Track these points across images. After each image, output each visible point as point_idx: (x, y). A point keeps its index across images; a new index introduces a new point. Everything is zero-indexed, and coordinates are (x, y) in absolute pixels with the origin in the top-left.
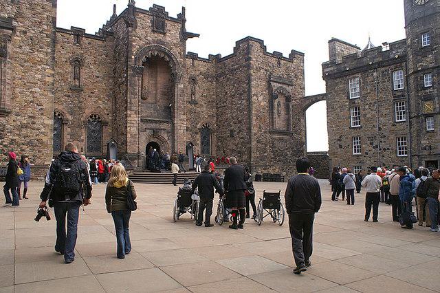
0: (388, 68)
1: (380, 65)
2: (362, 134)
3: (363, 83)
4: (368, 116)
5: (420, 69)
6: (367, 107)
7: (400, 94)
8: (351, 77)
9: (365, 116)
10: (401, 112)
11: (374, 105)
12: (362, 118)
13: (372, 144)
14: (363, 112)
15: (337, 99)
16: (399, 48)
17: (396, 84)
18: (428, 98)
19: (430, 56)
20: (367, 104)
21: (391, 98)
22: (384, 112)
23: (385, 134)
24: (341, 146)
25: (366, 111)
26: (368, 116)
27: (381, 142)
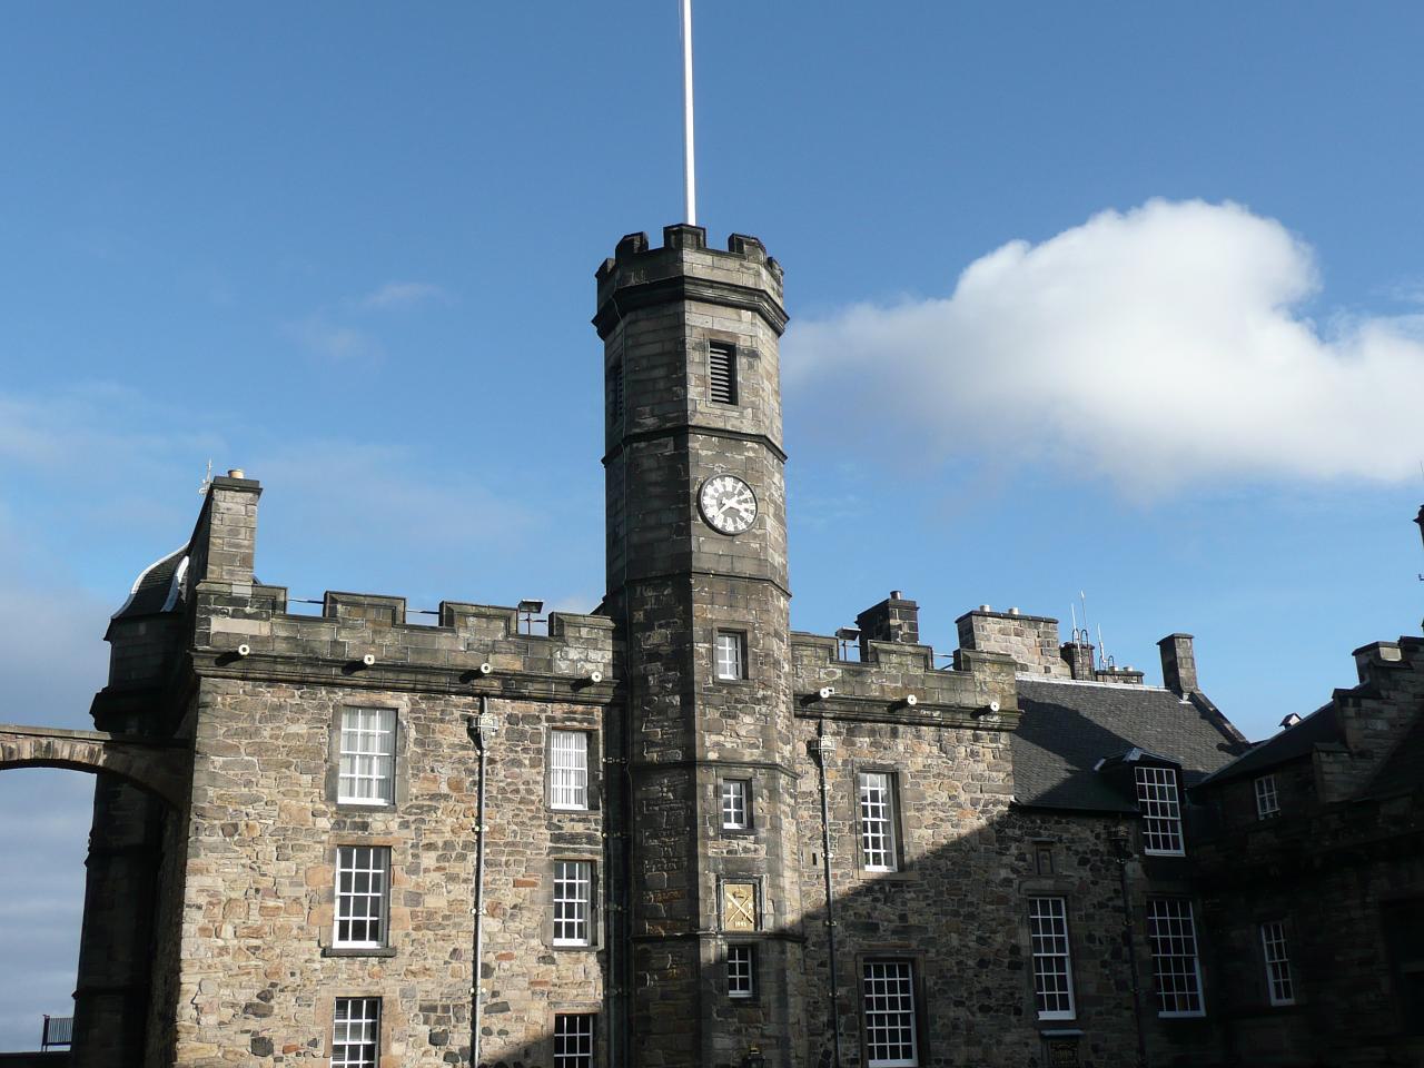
0: (534, 707)
1: (512, 687)
2: (389, 988)
3: (420, 743)
4: (431, 902)
5: (713, 756)
6: (429, 859)
7: (580, 828)
8: (361, 697)
9: (415, 898)
10: (570, 906)
11: (462, 857)
12: (399, 909)
13: (435, 1040)
14: (404, 883)
15: (266, 787)
16: (592, 643)
17: (558, 784)
18: (737, 872)
19: (748, 719)
20: (430, 847)
21: (543, 837)
22: (509, 897)
23: (508, 995)
24: (261, 1046)
25: (422, 879)
26: (431, 902)
27: (487, 1032)
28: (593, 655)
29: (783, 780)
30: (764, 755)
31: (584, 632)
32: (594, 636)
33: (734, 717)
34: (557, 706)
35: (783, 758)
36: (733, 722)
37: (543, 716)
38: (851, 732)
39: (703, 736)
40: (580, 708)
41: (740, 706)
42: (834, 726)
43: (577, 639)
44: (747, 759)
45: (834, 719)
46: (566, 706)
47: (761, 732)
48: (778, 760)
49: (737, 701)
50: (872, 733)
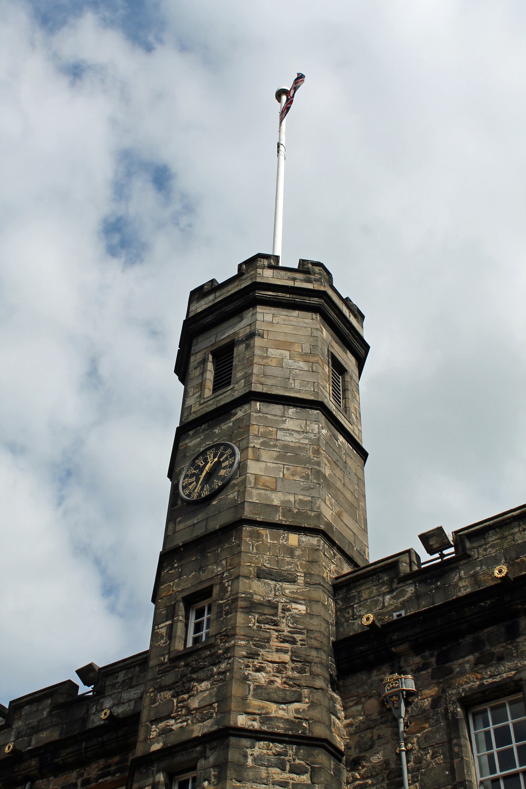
16: (128, 685)
28: (125, 696)
29: (260, 748)
30: (217, 722)
31: (121, 677)
32: (130, 675)
33: (188, 691)
34: (94, 766)
35: (266, 719)
36: (186, 696)
37: (79, 782)
38: (444, 659)
39: (148, 731)
40: (116, 759)
41: (194, 676)
42: (417, 660)
43: (113, 686)
44: (196, 734)
45: (417, 649)
46: (102, 762)
47: (216, 696)
48: (242, 721)
49: (194, 671)
50: (477, 646)
